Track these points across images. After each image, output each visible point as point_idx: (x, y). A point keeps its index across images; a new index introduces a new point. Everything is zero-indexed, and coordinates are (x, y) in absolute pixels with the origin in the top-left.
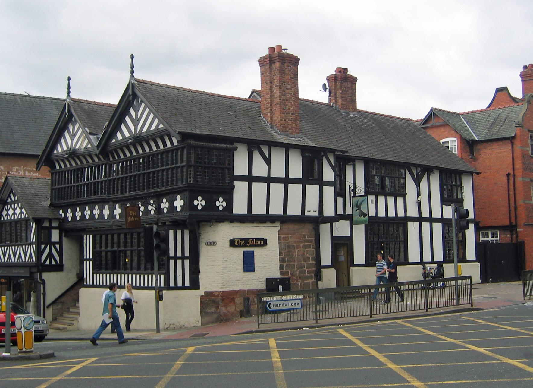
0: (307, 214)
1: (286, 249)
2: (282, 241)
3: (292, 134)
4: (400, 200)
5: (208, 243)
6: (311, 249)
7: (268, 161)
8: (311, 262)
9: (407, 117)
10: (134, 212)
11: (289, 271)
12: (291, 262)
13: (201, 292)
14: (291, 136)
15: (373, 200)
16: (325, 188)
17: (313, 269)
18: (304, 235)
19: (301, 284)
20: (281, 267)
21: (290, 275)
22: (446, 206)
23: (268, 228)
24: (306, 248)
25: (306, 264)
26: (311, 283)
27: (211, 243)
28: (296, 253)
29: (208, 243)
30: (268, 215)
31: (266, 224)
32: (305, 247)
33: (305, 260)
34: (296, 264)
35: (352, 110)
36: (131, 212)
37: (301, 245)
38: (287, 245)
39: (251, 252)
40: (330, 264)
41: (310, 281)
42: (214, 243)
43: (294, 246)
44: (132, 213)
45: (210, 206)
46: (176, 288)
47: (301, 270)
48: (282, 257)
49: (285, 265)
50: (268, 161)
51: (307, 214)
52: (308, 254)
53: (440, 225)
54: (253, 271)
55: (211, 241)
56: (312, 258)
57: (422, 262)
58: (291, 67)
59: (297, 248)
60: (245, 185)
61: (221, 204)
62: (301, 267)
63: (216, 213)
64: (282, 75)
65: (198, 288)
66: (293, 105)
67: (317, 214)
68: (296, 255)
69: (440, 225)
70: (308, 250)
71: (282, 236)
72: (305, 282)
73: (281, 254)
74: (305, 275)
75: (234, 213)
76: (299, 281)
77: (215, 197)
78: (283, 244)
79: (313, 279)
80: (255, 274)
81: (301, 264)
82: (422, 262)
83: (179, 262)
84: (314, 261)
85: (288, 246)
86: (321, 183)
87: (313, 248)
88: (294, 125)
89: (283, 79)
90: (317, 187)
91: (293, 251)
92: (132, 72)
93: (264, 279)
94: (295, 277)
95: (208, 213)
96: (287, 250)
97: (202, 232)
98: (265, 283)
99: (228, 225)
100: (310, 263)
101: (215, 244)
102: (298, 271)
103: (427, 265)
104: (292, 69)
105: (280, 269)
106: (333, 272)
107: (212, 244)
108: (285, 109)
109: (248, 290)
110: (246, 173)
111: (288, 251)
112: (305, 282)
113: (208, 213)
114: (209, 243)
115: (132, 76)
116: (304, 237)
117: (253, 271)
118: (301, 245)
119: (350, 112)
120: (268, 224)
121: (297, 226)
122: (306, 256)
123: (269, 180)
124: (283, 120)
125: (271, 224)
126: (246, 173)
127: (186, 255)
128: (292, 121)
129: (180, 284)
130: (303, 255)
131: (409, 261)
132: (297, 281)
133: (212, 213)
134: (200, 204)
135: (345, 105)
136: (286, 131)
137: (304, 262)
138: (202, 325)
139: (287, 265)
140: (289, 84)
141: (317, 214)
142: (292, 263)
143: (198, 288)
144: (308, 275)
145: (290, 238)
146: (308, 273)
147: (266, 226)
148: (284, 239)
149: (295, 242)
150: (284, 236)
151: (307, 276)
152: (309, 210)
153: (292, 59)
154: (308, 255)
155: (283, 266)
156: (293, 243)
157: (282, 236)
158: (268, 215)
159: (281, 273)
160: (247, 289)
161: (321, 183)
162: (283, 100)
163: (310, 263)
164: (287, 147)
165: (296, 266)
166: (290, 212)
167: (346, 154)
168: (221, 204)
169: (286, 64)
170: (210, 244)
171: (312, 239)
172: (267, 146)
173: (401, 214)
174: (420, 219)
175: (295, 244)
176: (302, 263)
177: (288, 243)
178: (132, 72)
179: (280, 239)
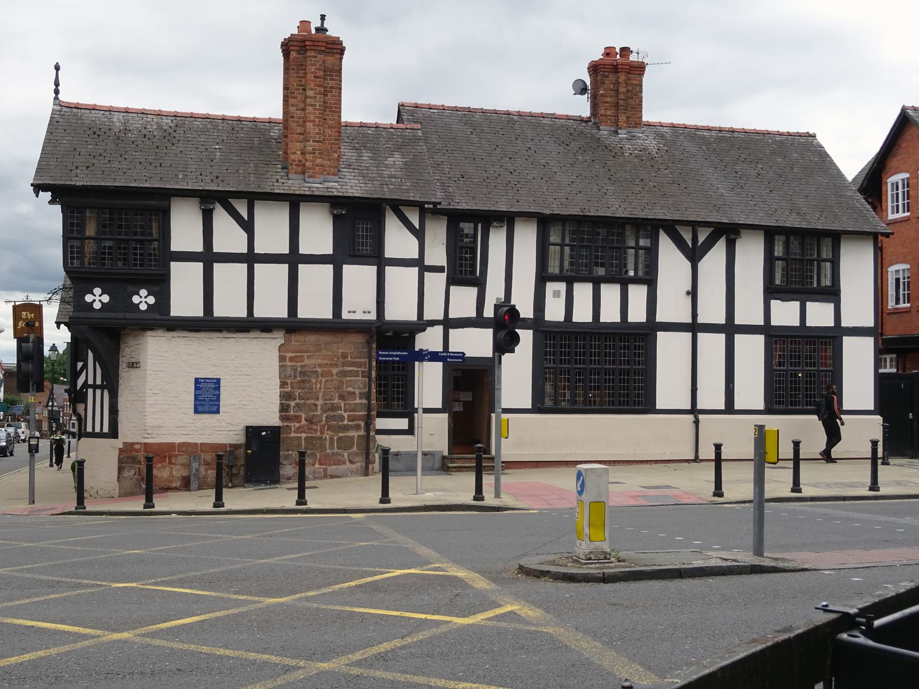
0: (345, 316)
1: (295, 377)
2: (288, 363)
3: (314, 177)
4: (638, 294)
5: (129, 363)
6: (360, 378)
7: (248, 226)
8: (358, 401)
9: (803, 130)
10: (31, 314)
11: (304, 416)
12: (308, 399)
13: (118, 443)
14: (311, 180)
15: (559, 292)
16: (391, 272)
17: (361, 413)
18: (342, 352)
19: (332, 440)
20: (284, 408)
21: (304, 422)
22: (782, 300)
23: (255, 340)
24: (345, 376)
25: (345, 404)
26: (356, 437)
27: (133, 363)
28: (319, 385)
29: (129, 364)
30: (293, 319)
31: (251, 333)
32: (343, 374)
33: (342, 397)
34: (320, 403)
35: (625, 125)
36: (24, 313)
37: (335, 371)
38: (299, 369)
39: (215, 381)
40: (439, 405)
41: (354, 434)
42: (137, 363)
43: (316, 371)
44: (27, 314)
45: (121, 302)
46: (93, 435)
47: (332, 414)
48: (289, 389)
49: (293, 404)
50: (248, 226)
51: (345, 316)
52: (350, 386)
53: (760, 340)
54: (218, 412)
55: (133, 360)
56: (360, 393)
57: (694, 410)
58: (316, 57)
59: (322, 375)
60: (198, 268)
61: (143, 300)
62: (334, 408)
63: (137, 316)
64: (297, 73)
65: (117, 438)
66: (318, 126)
67: (373, 316)
68: (320, 388)
69: (760, 340)
70: (350, 381)
71: (288, 355)
72: (341, 435)
73: (283, 384)
74: (341, 423)
75: (172, 314)
76: (327, 434)
77: (130, 288)
78: (289, 369)
79: (363, 431)
80: (220, 418)
81: (333, 404)
82: (694, 410)
83: (98, 392)
84: (366, 399)
85: (301, 372)
86: (380, 261)
87: (363, 376)
88: (318, 161)
89: (300, 81)
90: (372, 270)
91: (314, 381)
92: (57, 92)
93: (241, 427)
94: (316, 425)
95: (114, 315)
96: (299, 379)
97: (123, 346)
98: (243, 433)
99: (163, 335)
100: (354, 402)
101: (138, 366)
102: (325, 415)
103: (701, 417)
104: (317, 61)
105: (280, 412)
106: (443, 419)
107: (135, 366)
108: (303, 134)
109: (202, 444)
110: (199, 248)
111: (303, 381)
112: (341, 435)
113: (114, 315)
114: (131, 365)
115: (56, 98)
116: (344, 356)
117: (218, 412)
118: (335, 371)
119: (621, 129)
120: (257, 334)
121: (324, 338)
122: (345, 390)
123: (251, 258)
124: (299, 153)
125: (263, 334)
126: (199, 248)
127: (97, 384)
128: (314, 153)
129: (98, 430)
130: (338, 388)
131: (658, 407)
132: (322, 432)
133: (129, 315)
134: (97, 301)
135: (610, 116)
136: (304, 173)
137: (341, 401)
138: (119, 496)
139: (297, 404)
140: (312, 89)
141: (373, 316)
142: (312, 401)
143: (117, 438)
144: (350, 423)
145: (307, 359)
146: (349, 421)
147: (252, 336)
148: (291, 359)
149: (320, 365)
150: (293, 355)
151: (348, 424)
152: (367, 310)
153: (316, 44)
154: (350, 389)
155: (289, 406)
156: (315, 367)
157: (288, 355)
158: (250, 319)
159: (282, 418)
160: (199, 442)
161: (380, 261)
162: (300, 118)
163: (355, 404)
164: (295, 202)
165: (319, 407)
166: (303, 313)
167: (438, 207)
168: (143, 300)
169: (308, 54)
170: (133, 365)
171: (363, 360)
172: (246, 200)
173: (637, 314)
174: (694, 328)
175: (319, 370)
176: (336, 401)
177: (301, 367)
178: (57, 92)
179: (282, 359)
